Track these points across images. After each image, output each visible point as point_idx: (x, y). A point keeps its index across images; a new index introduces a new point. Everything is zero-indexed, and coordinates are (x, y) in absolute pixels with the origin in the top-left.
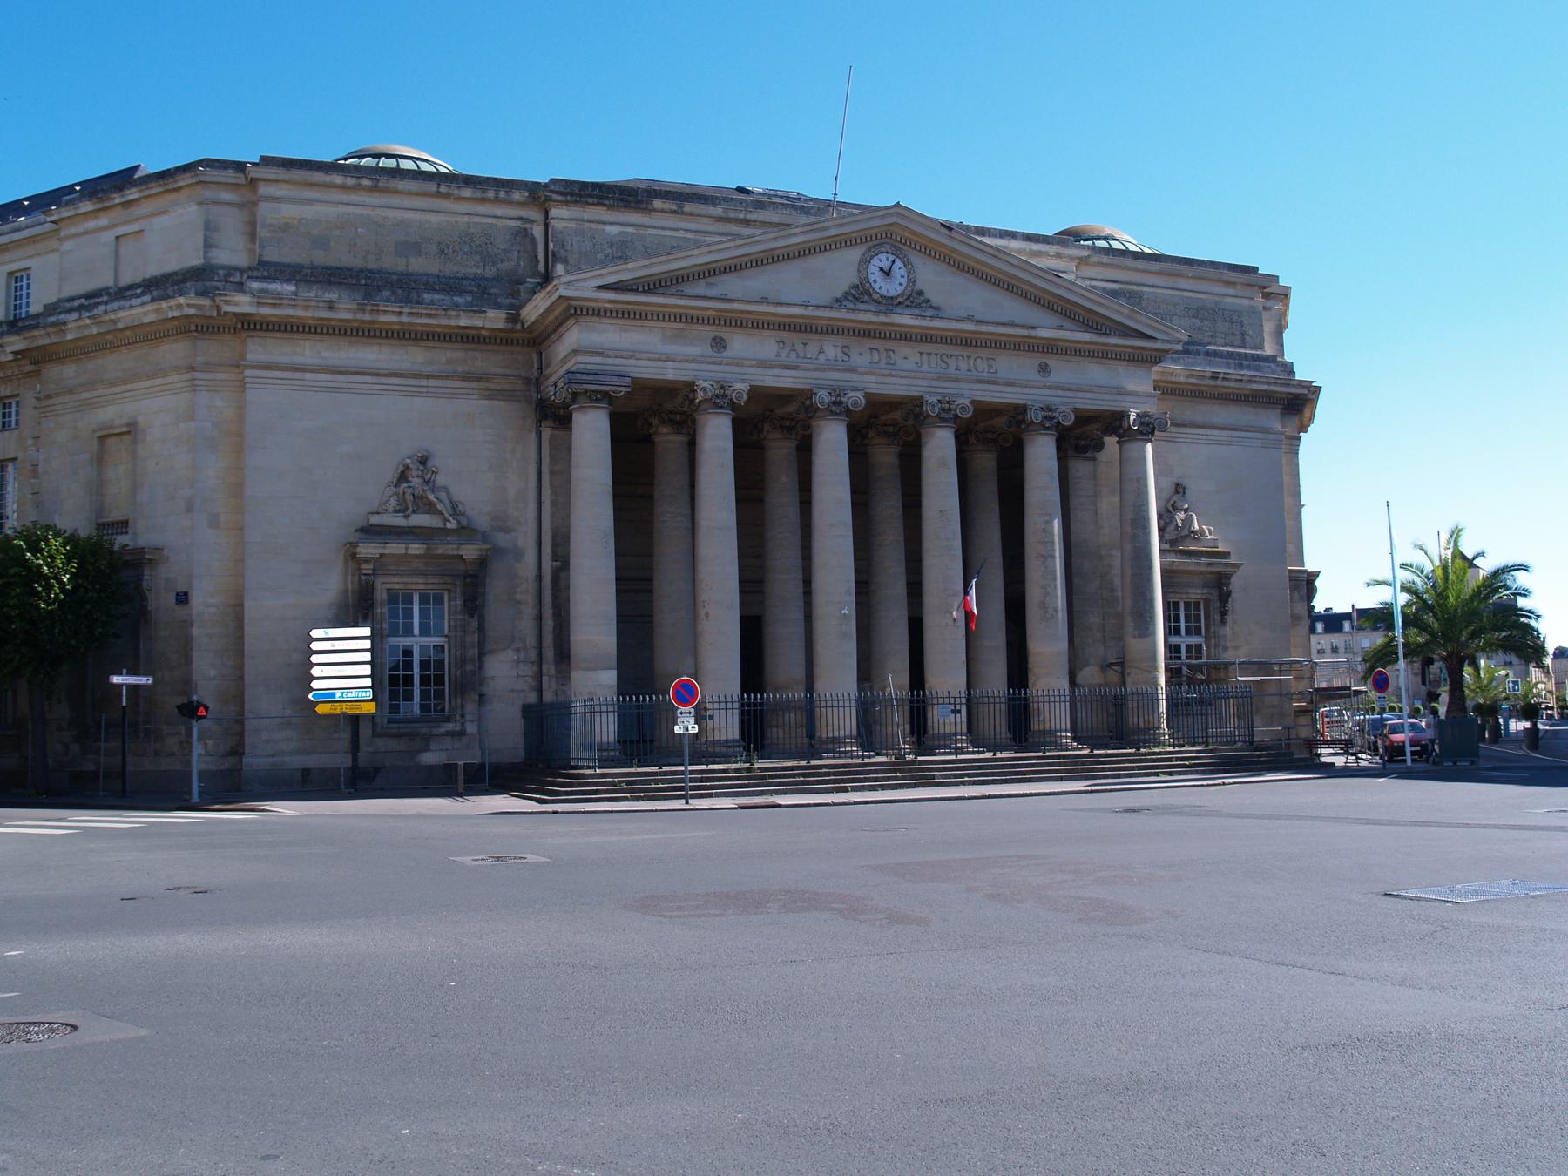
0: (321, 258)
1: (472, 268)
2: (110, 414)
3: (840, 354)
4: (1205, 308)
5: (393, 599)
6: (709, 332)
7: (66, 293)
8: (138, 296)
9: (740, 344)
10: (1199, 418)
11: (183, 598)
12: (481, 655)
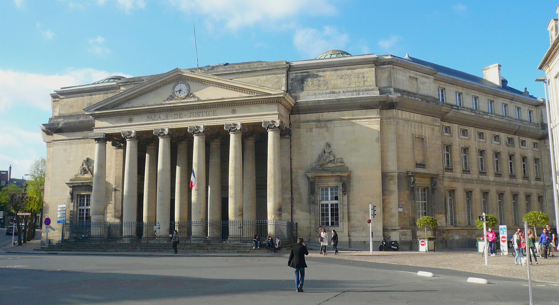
6: (128, 117)
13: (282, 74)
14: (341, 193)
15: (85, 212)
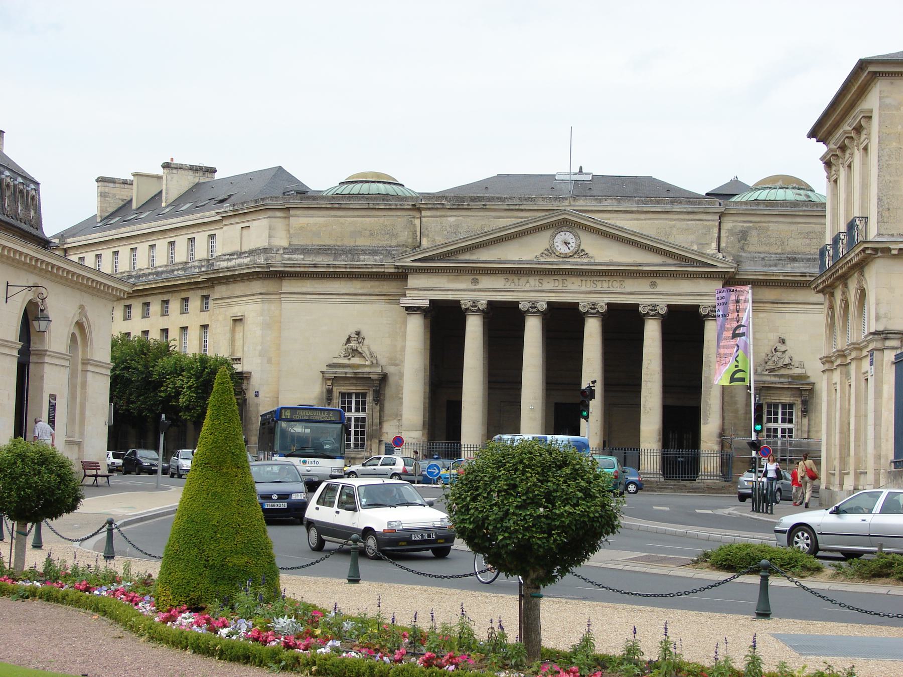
0: (317, 242)
1: (385, 242)
2: (237, 310)
3: (537, 283)
4: (815, 232)
5: (343, 395)
7: (224, 252)
8: (246, 257)
9: (486, 282)
10: (800, 299)
11: (257, 394)
12: (381, 423)
13: (713, 221)
14: (800, 414)
15: (353, 423)
